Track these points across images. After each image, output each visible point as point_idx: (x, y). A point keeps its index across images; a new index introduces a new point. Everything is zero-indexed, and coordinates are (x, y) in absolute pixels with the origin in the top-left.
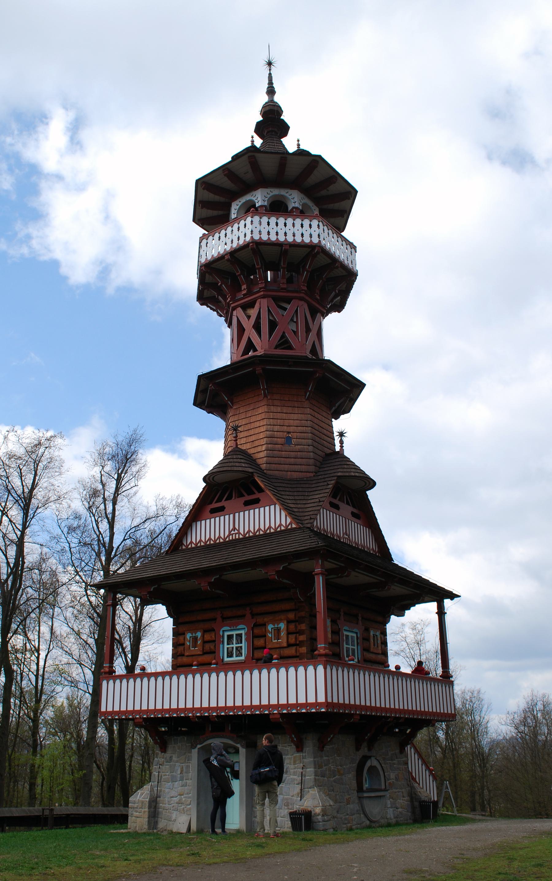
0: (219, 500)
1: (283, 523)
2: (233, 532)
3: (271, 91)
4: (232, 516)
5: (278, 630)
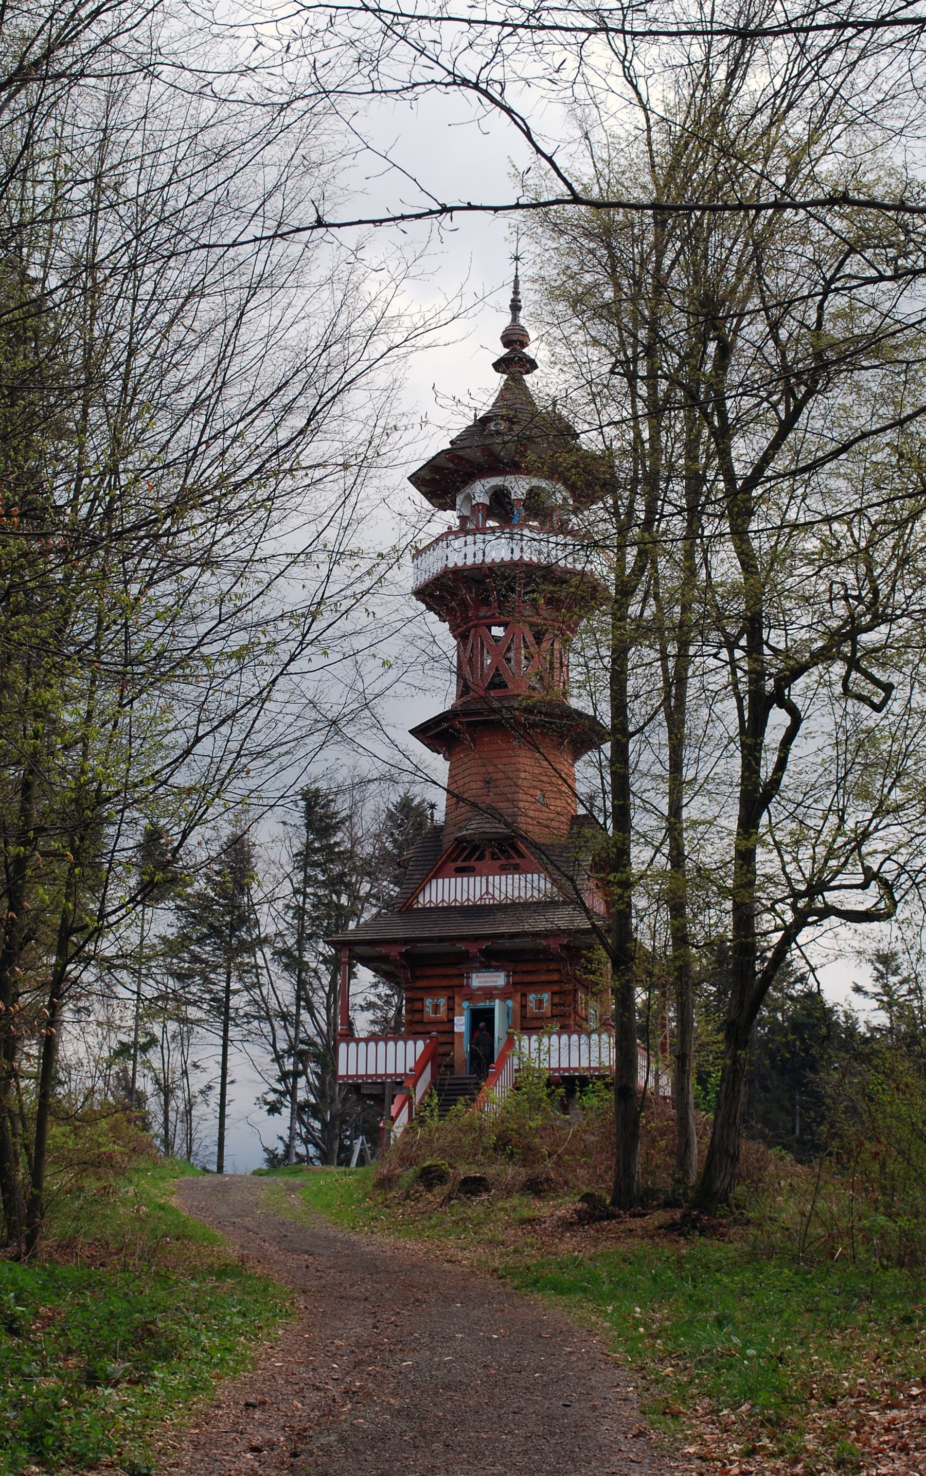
5: (540, 1003)
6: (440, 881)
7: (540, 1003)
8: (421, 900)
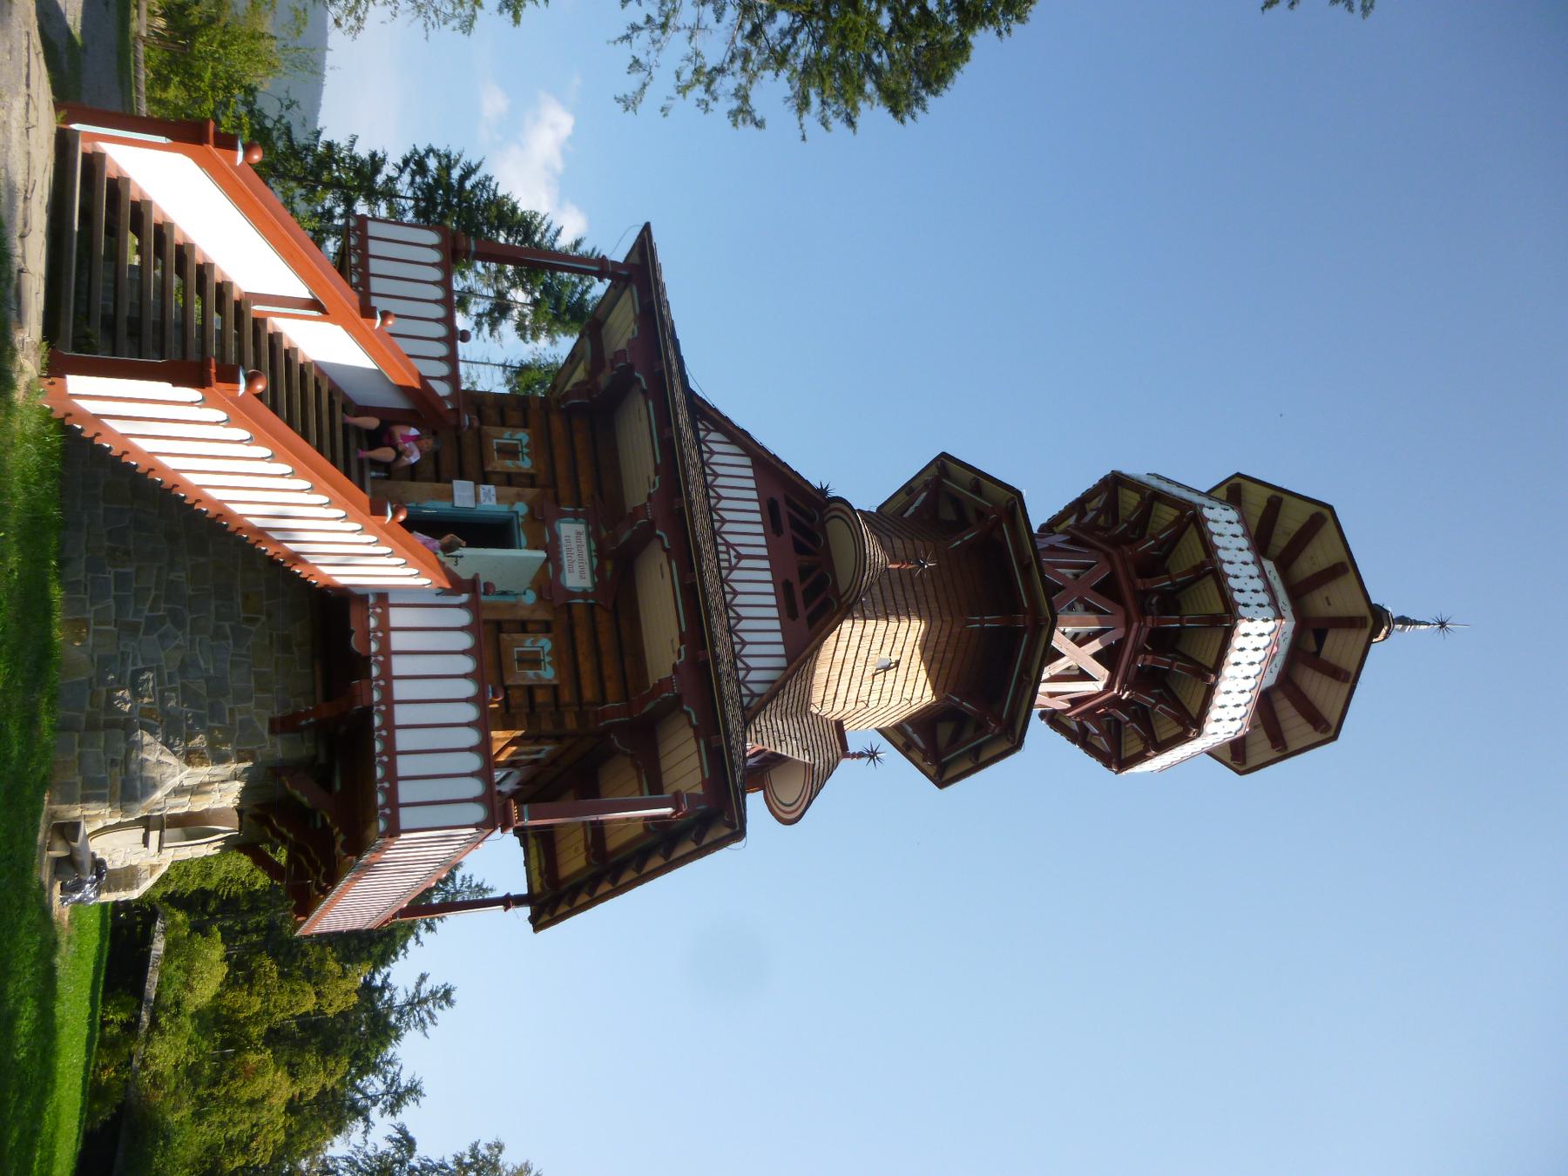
0: (796, 525)
1: (753, 676)
2: (732, 553)
3: (1404, 621)
4: (764, 552)
5: (533, 661)
6: (750, 472)
7: (533, 661)
8: (713, 436)
